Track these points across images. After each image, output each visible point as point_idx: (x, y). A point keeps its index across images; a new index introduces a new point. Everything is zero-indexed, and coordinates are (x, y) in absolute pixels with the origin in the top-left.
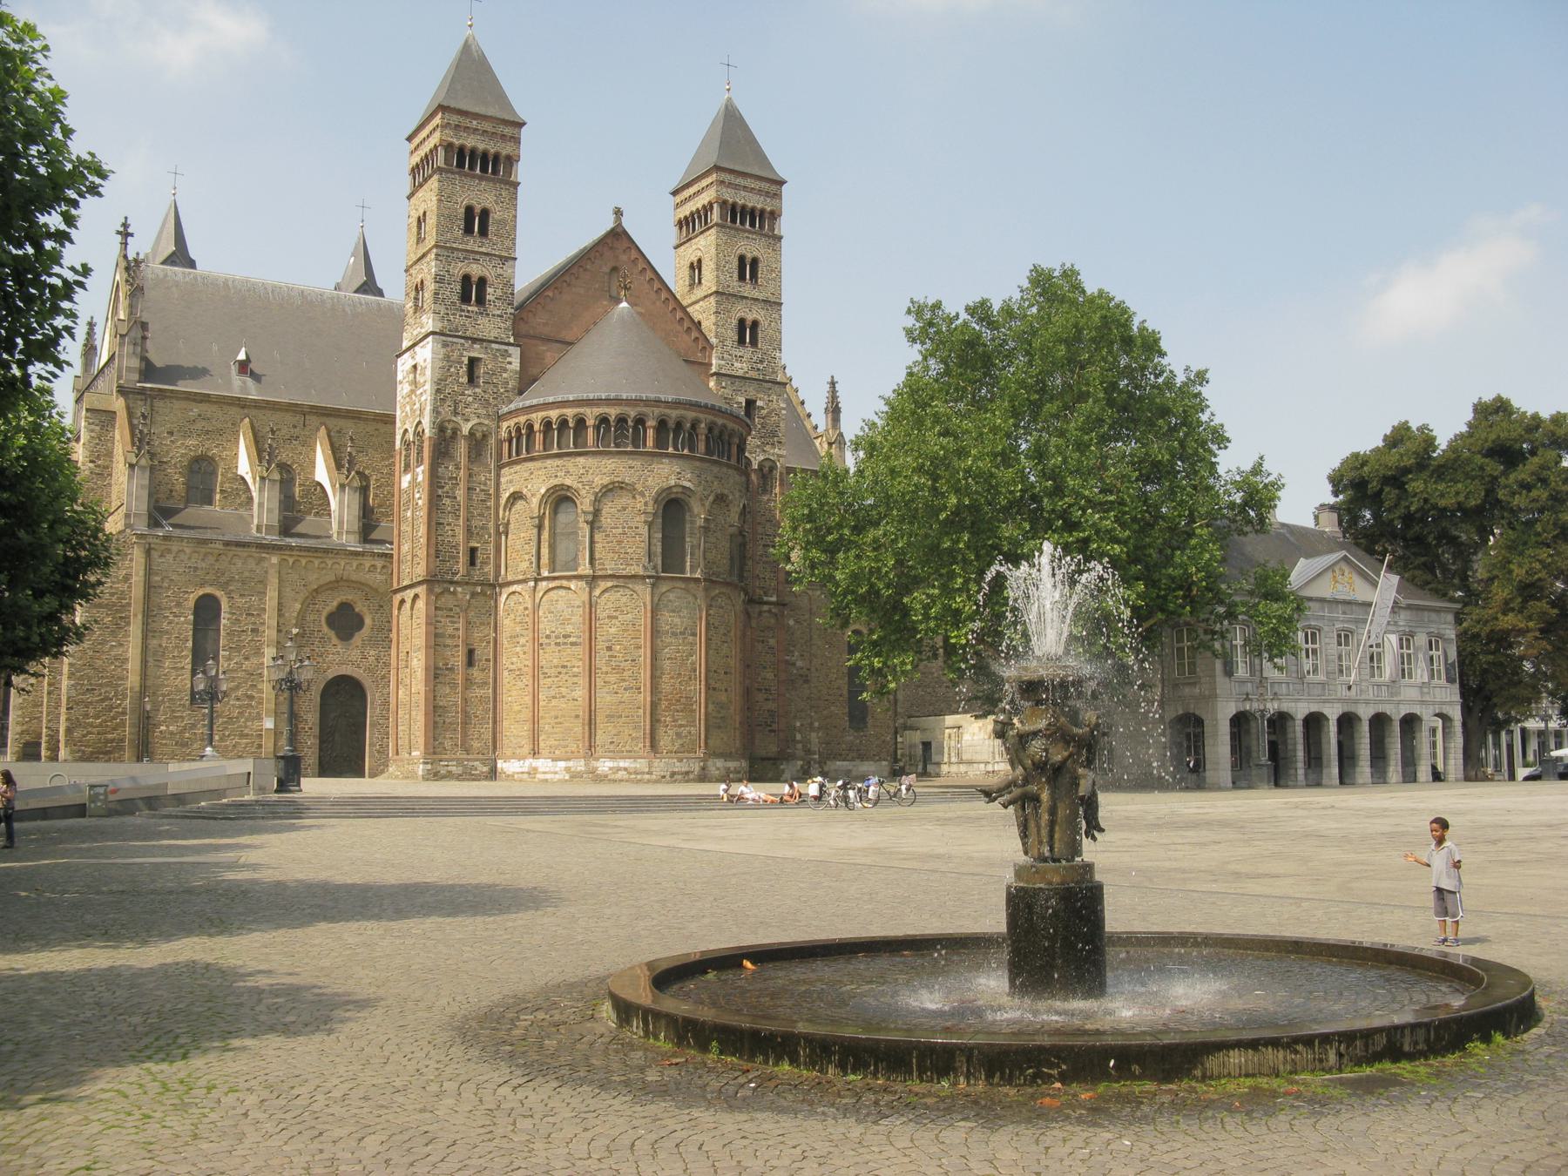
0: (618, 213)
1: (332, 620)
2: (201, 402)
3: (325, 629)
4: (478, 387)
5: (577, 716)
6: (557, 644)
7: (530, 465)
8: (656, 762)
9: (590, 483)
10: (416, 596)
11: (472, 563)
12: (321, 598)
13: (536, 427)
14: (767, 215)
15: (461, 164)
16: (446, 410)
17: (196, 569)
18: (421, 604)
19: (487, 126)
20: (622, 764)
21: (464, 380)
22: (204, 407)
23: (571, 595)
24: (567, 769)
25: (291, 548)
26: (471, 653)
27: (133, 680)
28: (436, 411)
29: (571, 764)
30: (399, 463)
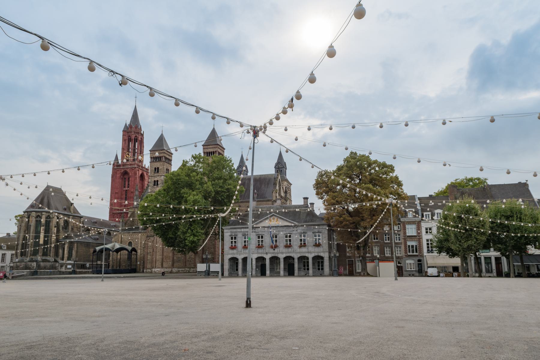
20: (158, 269)
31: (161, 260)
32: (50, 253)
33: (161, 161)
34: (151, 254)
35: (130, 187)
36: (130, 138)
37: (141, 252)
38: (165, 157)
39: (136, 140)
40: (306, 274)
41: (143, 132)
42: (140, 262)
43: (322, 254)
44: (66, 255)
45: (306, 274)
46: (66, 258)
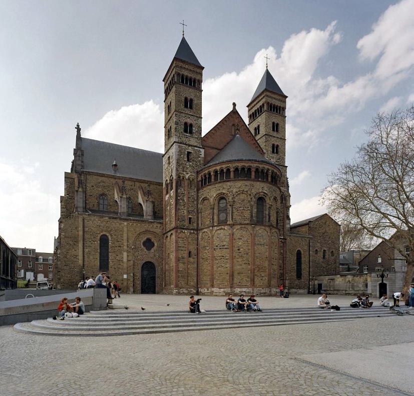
1: (144, 244)
2: (102, 176)
3: (142, 247)
4: (191, 162)
5: (227, 273)
6: (220, 249)
7: (210, 187)
8: (255, 289)
9: (232, 191)
10: (172, 234)
11: (190, 223)
12: (141, 236)
13: (212, 173)
14: (281, 109)
15: (183, 82)
16: (180, 170)
17: (100, 226)
18: (173, 237)
20: (244, 290)
21: (186, 159)
22: (103, 178)
23: (225, 232)
24: (224, 292)
25: (131, 220)
26: (190, 252)
27: (81, 262)
28: (177, 170)
29: (225, 290)
30: (164, 192)
37: (128, 256)
42: (127, 274)
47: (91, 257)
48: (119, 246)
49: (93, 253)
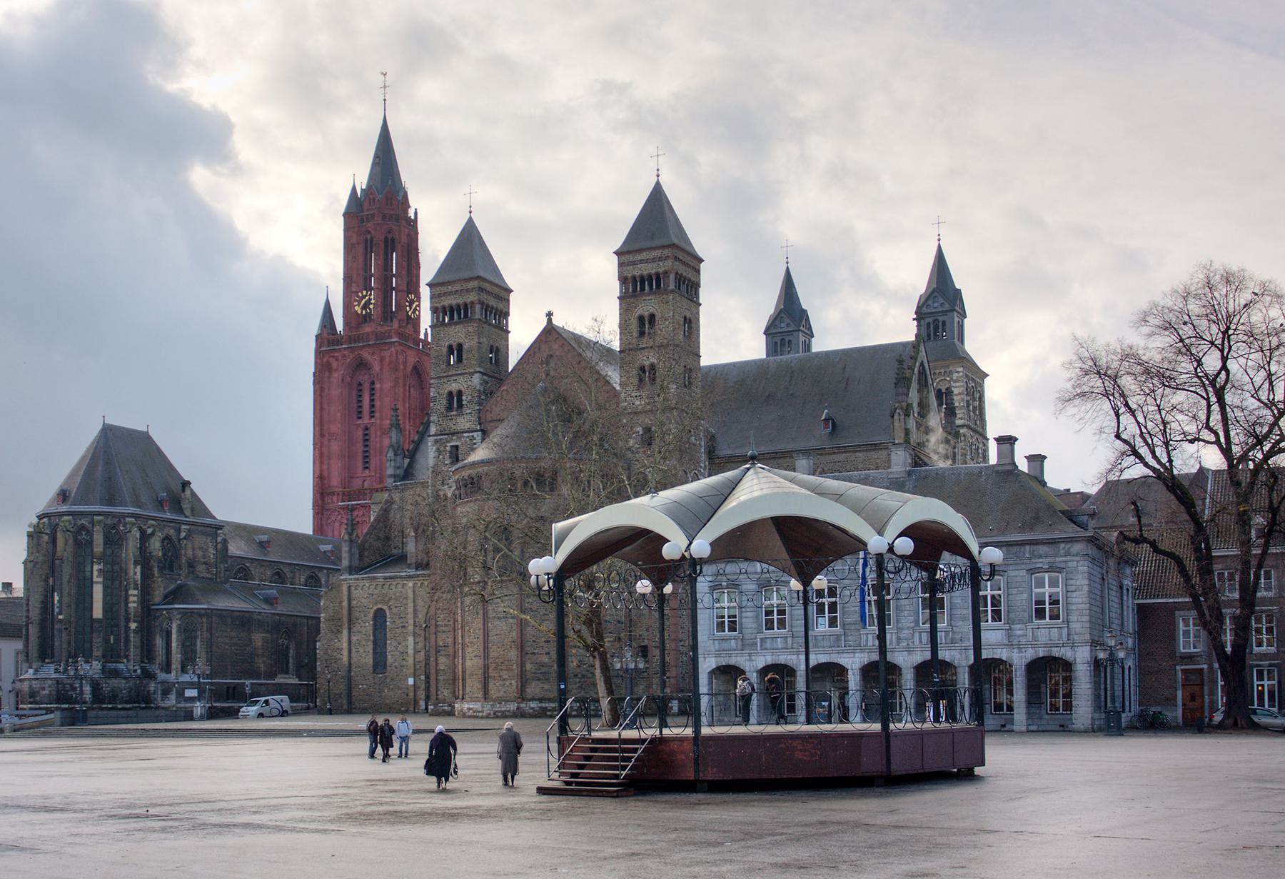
0: (550, 314)
19: (457, 287)
27: (345, 659)
31: (481, 672)
32: (127, 649)
33: (473, 320)
34: (451, 650)
35: (377, 415)
36: (372, 240)
37: (416, 643)
38: (481, 303)
39: (390, 245)
40: (1003, 726)
41: (416, 213)
42: (415, 675)
43: (1063, 650)
44: (176, 657)
45: (1003, 726)
46: (176, 665)
47: (361, 650)
48: (402, 627)
49: (364, 643)
